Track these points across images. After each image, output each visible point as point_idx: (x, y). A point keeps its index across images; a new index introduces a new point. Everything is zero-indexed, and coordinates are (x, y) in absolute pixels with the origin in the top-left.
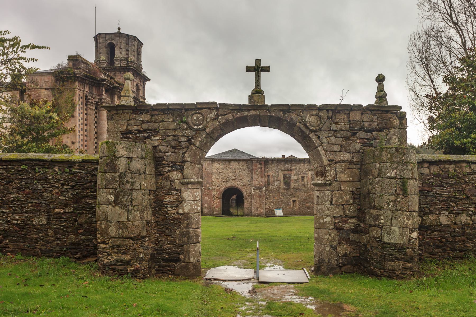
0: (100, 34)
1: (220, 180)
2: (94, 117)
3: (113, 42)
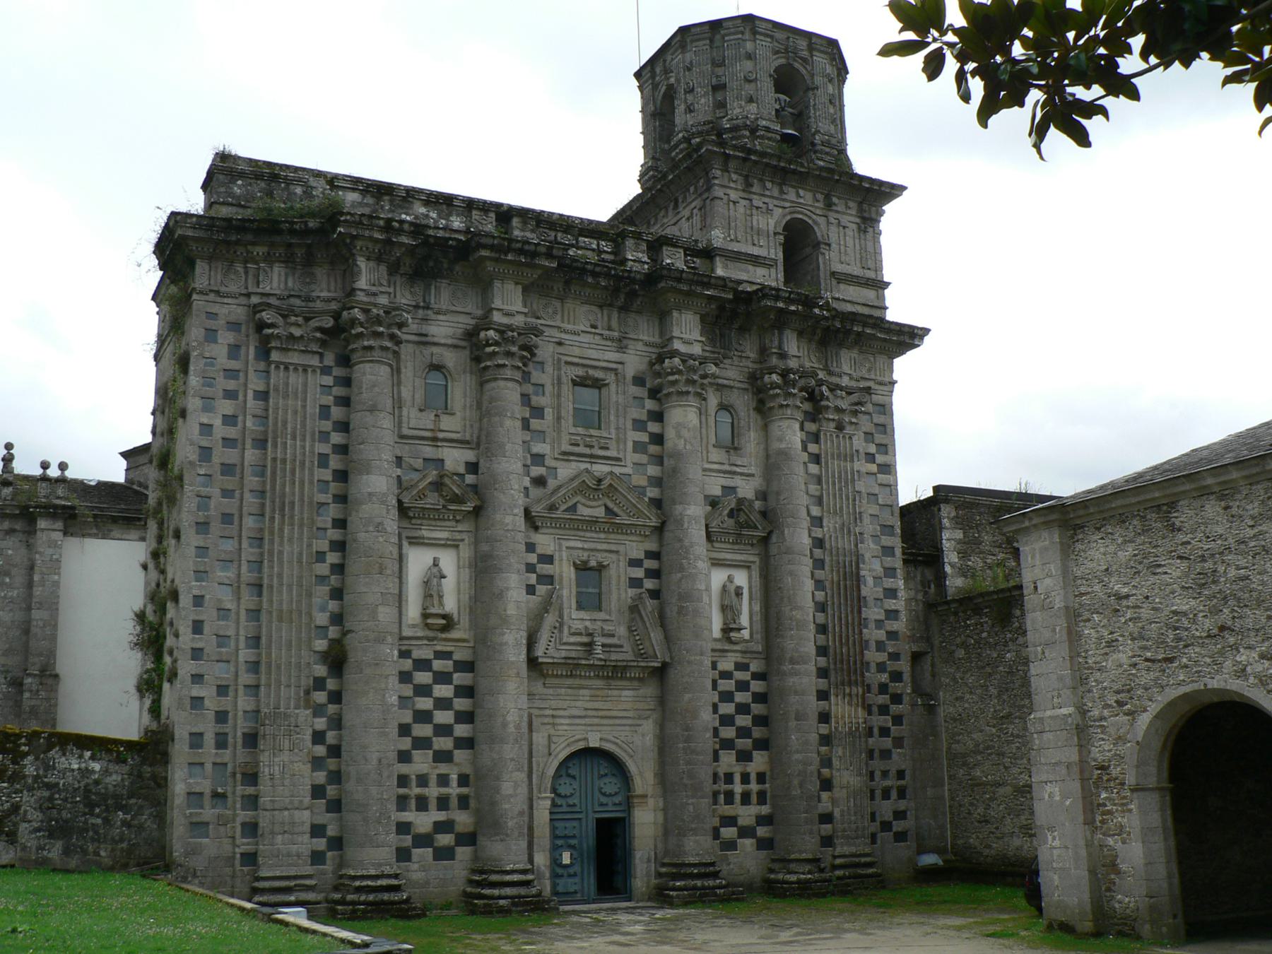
1: (1123, 656)
2: (329, 400)
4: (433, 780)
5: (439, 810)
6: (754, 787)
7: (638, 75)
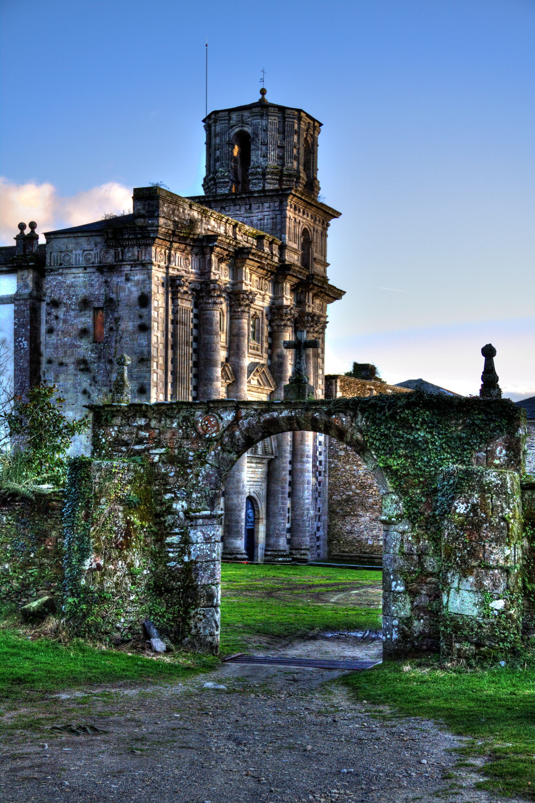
0: (215, 113)
2: (192, 325)
3: (246, 129)
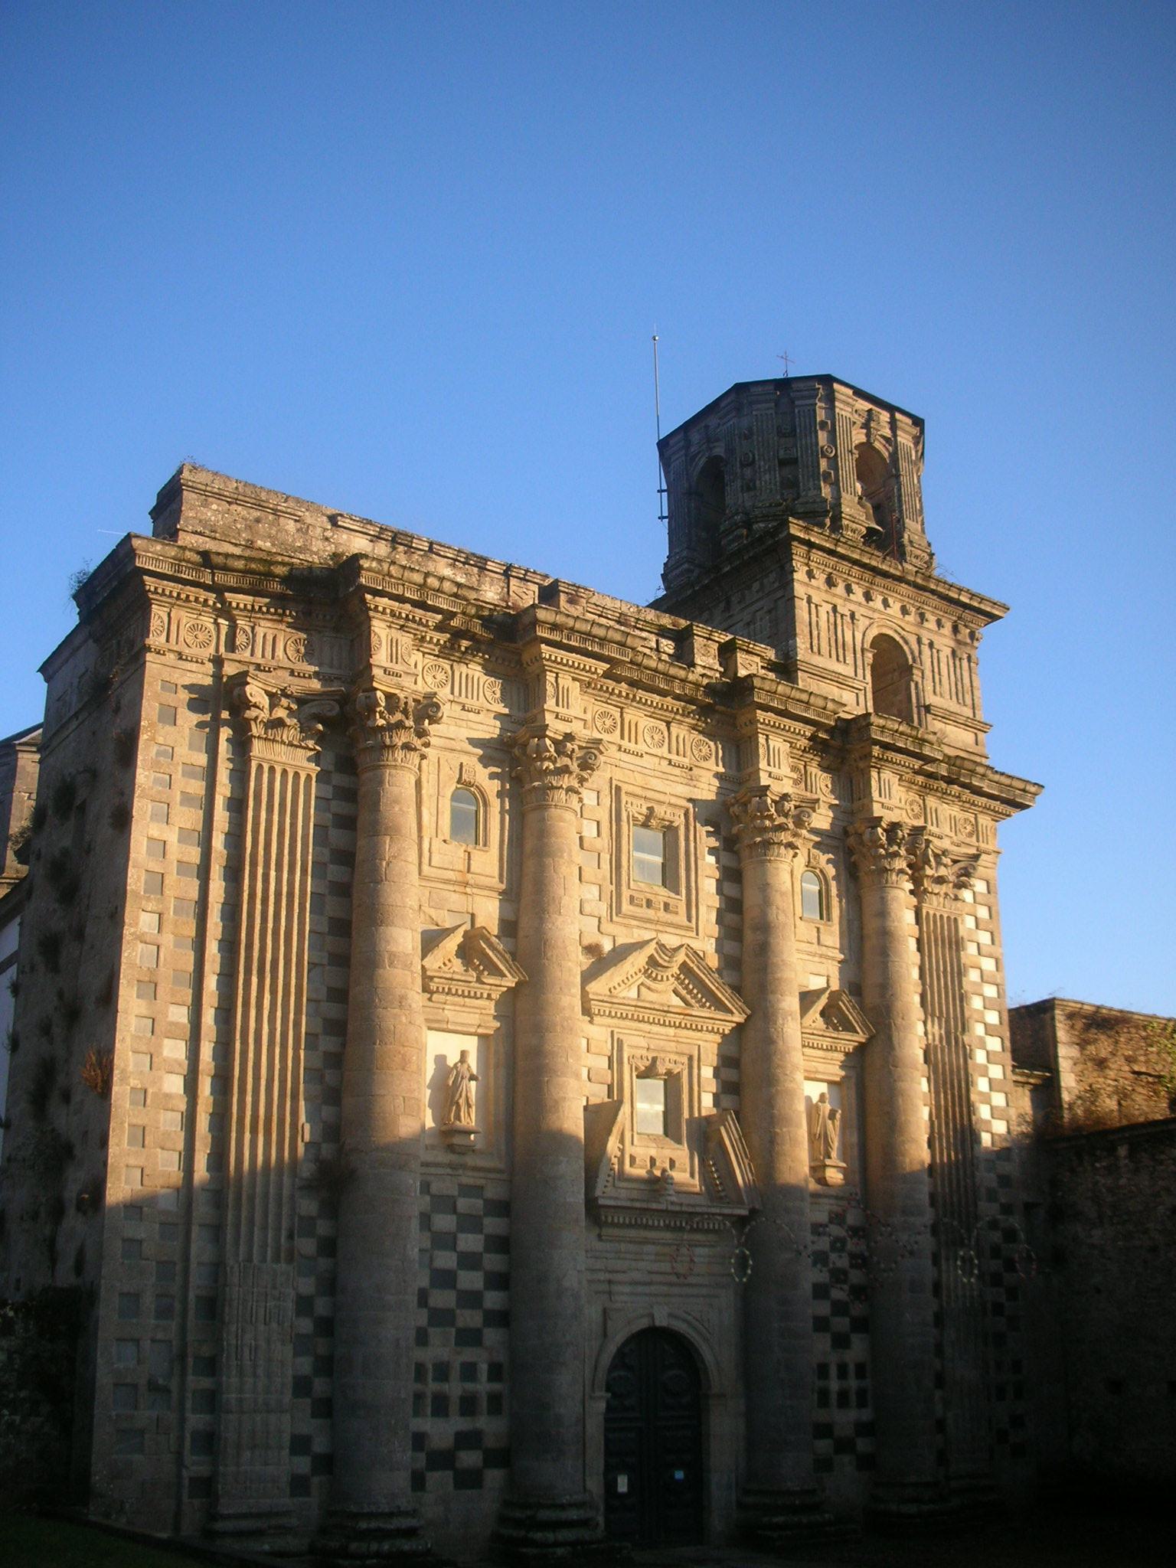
4: (455, 1373)
5: (463, 1414)
6: (853, 1383)
7: (663, 445)
